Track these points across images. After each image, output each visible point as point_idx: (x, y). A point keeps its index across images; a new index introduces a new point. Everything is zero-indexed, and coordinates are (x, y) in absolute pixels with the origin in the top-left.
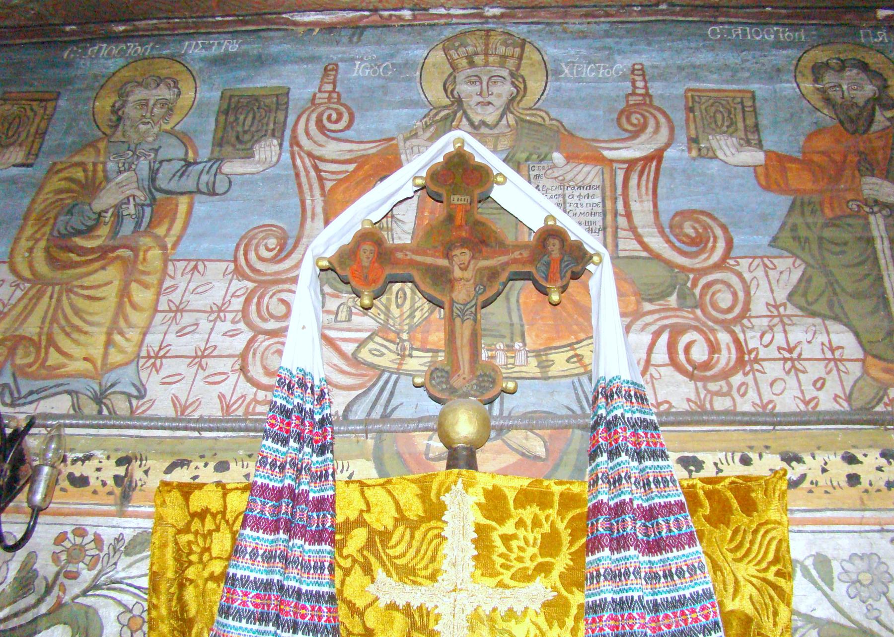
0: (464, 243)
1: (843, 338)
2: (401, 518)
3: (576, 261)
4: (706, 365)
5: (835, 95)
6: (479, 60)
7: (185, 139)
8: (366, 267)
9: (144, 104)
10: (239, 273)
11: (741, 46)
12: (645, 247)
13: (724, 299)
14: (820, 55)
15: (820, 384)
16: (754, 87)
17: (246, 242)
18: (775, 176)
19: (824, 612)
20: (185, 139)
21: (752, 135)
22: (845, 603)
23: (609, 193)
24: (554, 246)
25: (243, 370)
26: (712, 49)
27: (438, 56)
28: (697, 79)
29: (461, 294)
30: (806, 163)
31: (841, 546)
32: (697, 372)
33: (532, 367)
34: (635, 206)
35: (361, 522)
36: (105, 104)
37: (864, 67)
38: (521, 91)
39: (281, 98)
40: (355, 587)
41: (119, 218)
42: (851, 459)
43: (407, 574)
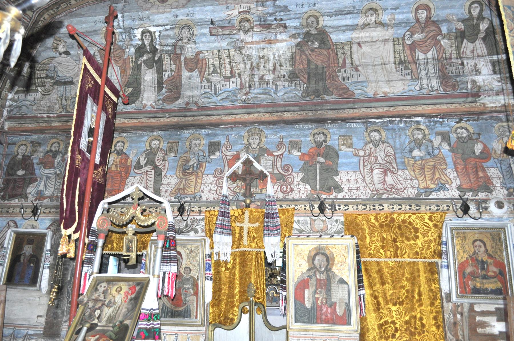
0: (248, 174)
2: (239, 215)
3: (266, 176)
4: (286, 191)
5: (316, 140)
6: (253, 134)
7: (203, 151)
8: (234, 177)
9: (195, 144)
10: (214, 176)
11: (301, 130)
12: (279, 171)
13: (290, 180)
14: (315, 131)
15: (303, 194)
16: (302, 139)
17: (215, 171)
18: (302, 157)
19: (298, 228)
20: (203, 151)
22: (301, 227)
23: (273, 162)
24: (262, 174)
25: (216, 193)
26: (295, 131)
27: (247, 134)
28: (292, 138)
29: (248, 182)
30: (308, 154)
31: (301, 218)
32: (284, 192)
33: (259, 192)
34: (278, 164)
35: (234, 215)
36: (188, 144)
37: (323, 133)
38: (261, 141)
39: (219, 142)
40: (233, 224)
41: (193, 167)
42: (305, 206)
43: (240, 222)
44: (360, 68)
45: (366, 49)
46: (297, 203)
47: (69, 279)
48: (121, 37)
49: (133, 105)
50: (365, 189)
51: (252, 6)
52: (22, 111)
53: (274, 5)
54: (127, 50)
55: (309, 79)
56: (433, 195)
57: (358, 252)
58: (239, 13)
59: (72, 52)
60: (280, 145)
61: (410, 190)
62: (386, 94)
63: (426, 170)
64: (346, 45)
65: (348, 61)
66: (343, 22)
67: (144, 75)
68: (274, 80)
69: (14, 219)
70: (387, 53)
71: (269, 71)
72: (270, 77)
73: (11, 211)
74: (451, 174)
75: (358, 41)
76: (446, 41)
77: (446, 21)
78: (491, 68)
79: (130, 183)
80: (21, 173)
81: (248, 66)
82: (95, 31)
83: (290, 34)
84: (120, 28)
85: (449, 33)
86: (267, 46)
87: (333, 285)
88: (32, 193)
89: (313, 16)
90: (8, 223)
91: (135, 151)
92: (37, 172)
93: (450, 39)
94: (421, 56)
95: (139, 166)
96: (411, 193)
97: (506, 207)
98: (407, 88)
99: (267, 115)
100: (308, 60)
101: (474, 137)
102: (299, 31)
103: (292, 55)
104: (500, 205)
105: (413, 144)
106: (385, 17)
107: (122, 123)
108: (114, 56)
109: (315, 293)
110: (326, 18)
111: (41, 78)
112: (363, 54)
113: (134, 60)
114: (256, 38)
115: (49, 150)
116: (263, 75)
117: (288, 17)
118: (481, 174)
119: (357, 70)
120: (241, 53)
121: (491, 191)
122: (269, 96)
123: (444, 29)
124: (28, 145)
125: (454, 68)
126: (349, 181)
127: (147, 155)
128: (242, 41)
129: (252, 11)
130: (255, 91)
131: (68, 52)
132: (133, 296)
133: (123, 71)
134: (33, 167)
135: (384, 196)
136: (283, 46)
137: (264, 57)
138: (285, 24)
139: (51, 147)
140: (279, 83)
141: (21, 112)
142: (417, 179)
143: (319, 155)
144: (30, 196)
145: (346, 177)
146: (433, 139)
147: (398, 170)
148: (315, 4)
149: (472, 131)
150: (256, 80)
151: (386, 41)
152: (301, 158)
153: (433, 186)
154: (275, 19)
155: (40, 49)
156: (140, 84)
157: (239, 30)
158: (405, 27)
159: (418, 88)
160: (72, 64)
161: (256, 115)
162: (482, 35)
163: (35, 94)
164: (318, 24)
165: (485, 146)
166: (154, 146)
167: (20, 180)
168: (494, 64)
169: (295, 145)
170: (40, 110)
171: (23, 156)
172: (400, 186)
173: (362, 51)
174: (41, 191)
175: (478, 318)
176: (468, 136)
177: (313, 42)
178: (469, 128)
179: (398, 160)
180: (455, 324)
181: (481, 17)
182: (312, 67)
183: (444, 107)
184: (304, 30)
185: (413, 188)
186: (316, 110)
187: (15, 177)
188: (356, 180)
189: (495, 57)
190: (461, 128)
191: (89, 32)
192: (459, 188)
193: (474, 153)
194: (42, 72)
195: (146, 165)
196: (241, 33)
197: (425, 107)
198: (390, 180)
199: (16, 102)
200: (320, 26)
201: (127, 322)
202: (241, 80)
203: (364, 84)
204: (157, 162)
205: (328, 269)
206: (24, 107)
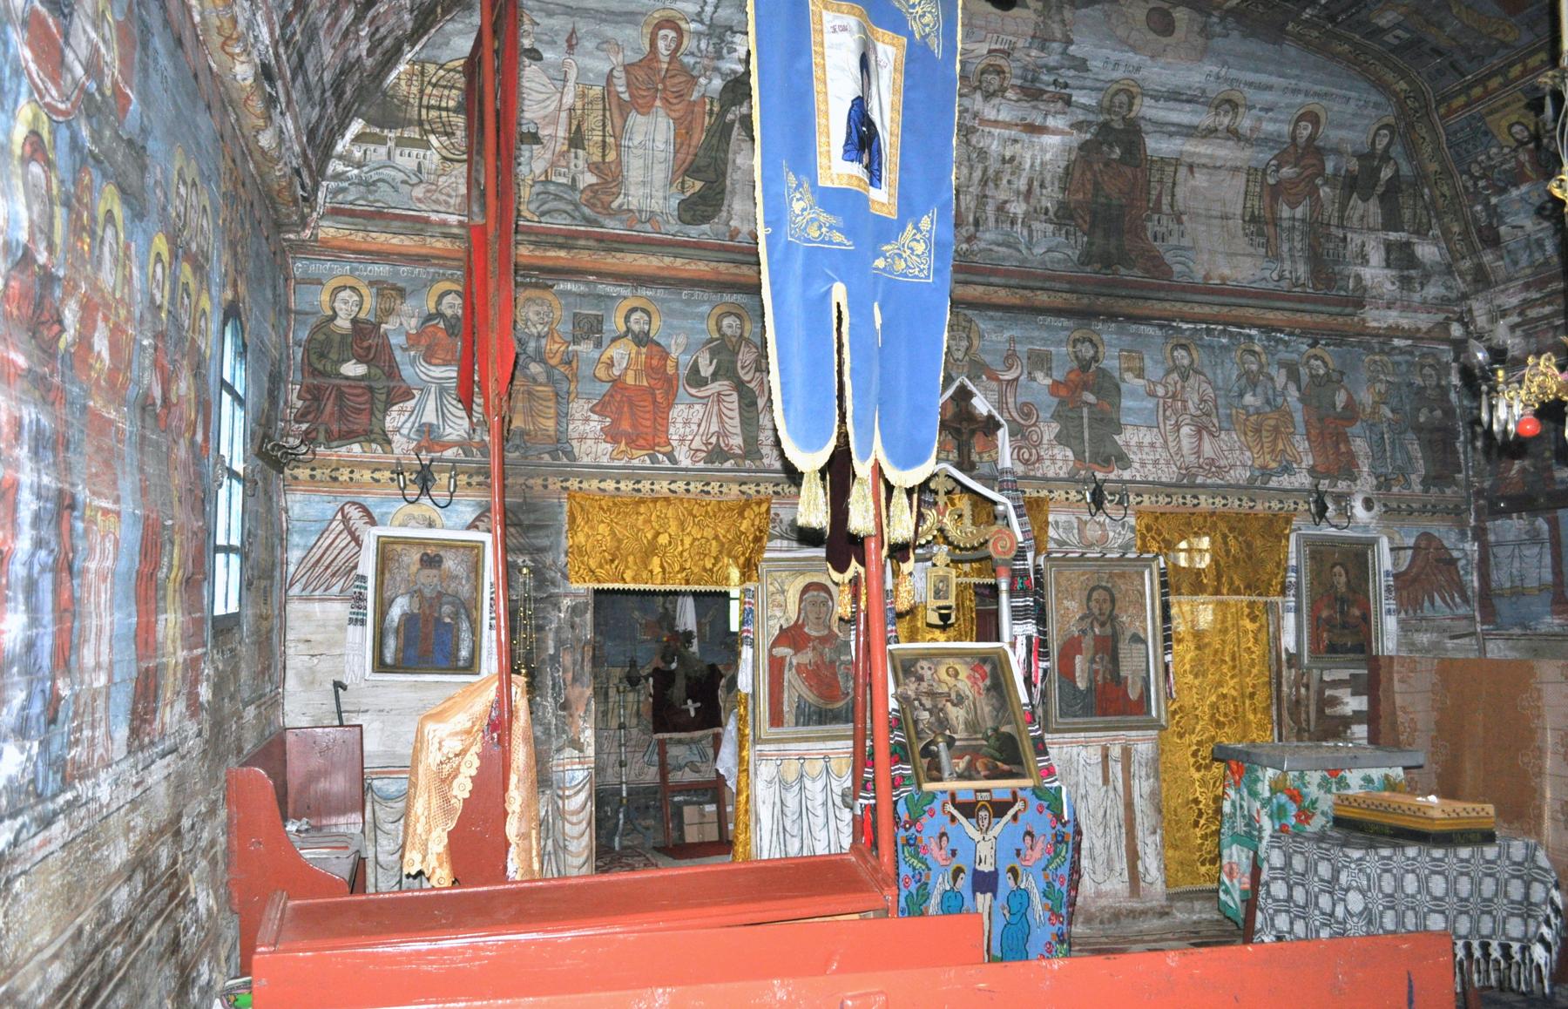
1: (1070, 453)
11: (1049, 328)
14: (1077, 335)
21: (1048, 374)
29: (965, 437)
30: (1065, 384)
31: (1062, 518)
32: (1026, 463)
37: (1091, 341)
44: (1185, 218)
45: (1200, 180)
46: (1052, 485)
47: (551, 651)
48: (694, 43)
49: (705, 227)
50: (1168, 463)
51: (1020, 44)
52: (377, 196)
53: (1064, 52)
54: (702, 81)
55: (1093, 225)
56: (1274, 483)
57: (1164, 584)
58: (990, 52)
59: (548, 55)
60: (1010, 359)
61: (1240, 470)
62: (1224, 279)
63: (1264, 433)
64: (1169, 164)
65: (1166, 200)
66: (1175, 117)
67: (735, 153)
68: (1026, 214)
69: (359, 499)
70: (1232, 193)
71: (1018, 193)
72: (1018, 208)
73: (344, 475)
74: (1302, 445)
75: (1189, 160)
76: (1327, 189)
77: (1337, 152)
78: (1383, 254)
79: (680, 420)
80: (353, 369)
81: (977, 174)
82: (632, 13)
83: (1074, 119)
84: (701, 22)
85: (1335, 175)
86: (1024, 136)
87: (1121, 645)
88: (405, 431)
89: (1126, 91)
90: (342, 509)
91: (682, 340)
92: (407, 372)
93: (1333, 187)
94: (1286, 212)
95: (696, 379)
96: (1240, 475)
97: (1376, 508)
98: (1259, 275)
99: (1002, 293)
100: (1097, 186)
101: (1335, 376)
102: (1091, 117)
103: (1067, 167)
104: (1368, 505)
105: (1243, 381)
106: (1245, 123)
107: (668, 267)
108: (665, 89)
109: (1093, 661)
110: (1148, 101)
111: (439, 108)
112: (1194, 190)
113: (716, 109)
114: (1004, 116)
115: (433, 311)
116: (1006, 202)
117: (1078, 83)
118: (1343, 448)
119: (1180, 222)
120: (968, 143)
121: (1354, 480)
122: (1015, 253)
123: (1330, 166)
124: (365, 291)
125: (1331, 246)
126: (1140, 445)
127: (714, 353)
128: (975, 115)
129: (1017, 55)
130: (988, 236)
131: (536, 51)
132: (988, 682)
133: (684, 128)
134: (392, 358)
135: (1199, 480)
136: (1052, 146)
137: (1012, 159)
138: (1070, 96)
139: (439, 302)
140: (1036, 225)
141: (371, 198)
142: (1249, 449)
143: (1086, 387)
144: (396, 438)
145: (1135, 439)
146: (1273, 371)
147: (1221, 429)
148: (1138, 69)
149: (1331, 365)
150: (990, 209)
151: (1236, 169)
152: (1055, 388)
153: (1273, 465)
154: (1055, 83)
155: (449, 27)
156: (724, 174)
157: (975, 89)
158: (1272, 148)
159: (1275, 276)
160: (543, 89)
161: (980, 289)
162: (1380, 190)
163: (422, 152)
164: (1130, 110)
165: (1350, 397)
166: (729, 332)
167: (359, 391)
168: (1389, 247)
169: (1040, 361)
170: (437, 202)
171: (354, 321)
172: (1223, 463)
173: (1192, 182)
174: (431, 425)
175: (1328, 693)
176: (1327, 374)
177: (1111, 146)
178: (1327, 358)
179: (1221, 411)
180: (1298, 702)
181: (1386, 157)
182: (1102, 200)
183: (1307, 318)
184: (1101, 118)
185: (1244, 466)
186: (1098, 295)
187: (337, 381)
188: (1152, 445)
189: (1393, 236)
190: (1316, 357)
191: (613, 13)
192: (1312, 471)
193: (1334, 406)
194: (446, 92)
195: (715, 376)
196: (978, 96)
197: (1279, 315)
198: (1208, 448)
199: (359, 166)
200: (1132, 115)
201: (1005, 729)
202: (958, 204)
203: (1189, 254)
204: (741, 373)
205: (1112, 618)
206: (383, 187)
